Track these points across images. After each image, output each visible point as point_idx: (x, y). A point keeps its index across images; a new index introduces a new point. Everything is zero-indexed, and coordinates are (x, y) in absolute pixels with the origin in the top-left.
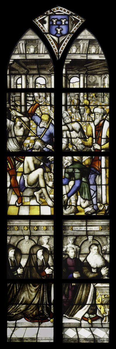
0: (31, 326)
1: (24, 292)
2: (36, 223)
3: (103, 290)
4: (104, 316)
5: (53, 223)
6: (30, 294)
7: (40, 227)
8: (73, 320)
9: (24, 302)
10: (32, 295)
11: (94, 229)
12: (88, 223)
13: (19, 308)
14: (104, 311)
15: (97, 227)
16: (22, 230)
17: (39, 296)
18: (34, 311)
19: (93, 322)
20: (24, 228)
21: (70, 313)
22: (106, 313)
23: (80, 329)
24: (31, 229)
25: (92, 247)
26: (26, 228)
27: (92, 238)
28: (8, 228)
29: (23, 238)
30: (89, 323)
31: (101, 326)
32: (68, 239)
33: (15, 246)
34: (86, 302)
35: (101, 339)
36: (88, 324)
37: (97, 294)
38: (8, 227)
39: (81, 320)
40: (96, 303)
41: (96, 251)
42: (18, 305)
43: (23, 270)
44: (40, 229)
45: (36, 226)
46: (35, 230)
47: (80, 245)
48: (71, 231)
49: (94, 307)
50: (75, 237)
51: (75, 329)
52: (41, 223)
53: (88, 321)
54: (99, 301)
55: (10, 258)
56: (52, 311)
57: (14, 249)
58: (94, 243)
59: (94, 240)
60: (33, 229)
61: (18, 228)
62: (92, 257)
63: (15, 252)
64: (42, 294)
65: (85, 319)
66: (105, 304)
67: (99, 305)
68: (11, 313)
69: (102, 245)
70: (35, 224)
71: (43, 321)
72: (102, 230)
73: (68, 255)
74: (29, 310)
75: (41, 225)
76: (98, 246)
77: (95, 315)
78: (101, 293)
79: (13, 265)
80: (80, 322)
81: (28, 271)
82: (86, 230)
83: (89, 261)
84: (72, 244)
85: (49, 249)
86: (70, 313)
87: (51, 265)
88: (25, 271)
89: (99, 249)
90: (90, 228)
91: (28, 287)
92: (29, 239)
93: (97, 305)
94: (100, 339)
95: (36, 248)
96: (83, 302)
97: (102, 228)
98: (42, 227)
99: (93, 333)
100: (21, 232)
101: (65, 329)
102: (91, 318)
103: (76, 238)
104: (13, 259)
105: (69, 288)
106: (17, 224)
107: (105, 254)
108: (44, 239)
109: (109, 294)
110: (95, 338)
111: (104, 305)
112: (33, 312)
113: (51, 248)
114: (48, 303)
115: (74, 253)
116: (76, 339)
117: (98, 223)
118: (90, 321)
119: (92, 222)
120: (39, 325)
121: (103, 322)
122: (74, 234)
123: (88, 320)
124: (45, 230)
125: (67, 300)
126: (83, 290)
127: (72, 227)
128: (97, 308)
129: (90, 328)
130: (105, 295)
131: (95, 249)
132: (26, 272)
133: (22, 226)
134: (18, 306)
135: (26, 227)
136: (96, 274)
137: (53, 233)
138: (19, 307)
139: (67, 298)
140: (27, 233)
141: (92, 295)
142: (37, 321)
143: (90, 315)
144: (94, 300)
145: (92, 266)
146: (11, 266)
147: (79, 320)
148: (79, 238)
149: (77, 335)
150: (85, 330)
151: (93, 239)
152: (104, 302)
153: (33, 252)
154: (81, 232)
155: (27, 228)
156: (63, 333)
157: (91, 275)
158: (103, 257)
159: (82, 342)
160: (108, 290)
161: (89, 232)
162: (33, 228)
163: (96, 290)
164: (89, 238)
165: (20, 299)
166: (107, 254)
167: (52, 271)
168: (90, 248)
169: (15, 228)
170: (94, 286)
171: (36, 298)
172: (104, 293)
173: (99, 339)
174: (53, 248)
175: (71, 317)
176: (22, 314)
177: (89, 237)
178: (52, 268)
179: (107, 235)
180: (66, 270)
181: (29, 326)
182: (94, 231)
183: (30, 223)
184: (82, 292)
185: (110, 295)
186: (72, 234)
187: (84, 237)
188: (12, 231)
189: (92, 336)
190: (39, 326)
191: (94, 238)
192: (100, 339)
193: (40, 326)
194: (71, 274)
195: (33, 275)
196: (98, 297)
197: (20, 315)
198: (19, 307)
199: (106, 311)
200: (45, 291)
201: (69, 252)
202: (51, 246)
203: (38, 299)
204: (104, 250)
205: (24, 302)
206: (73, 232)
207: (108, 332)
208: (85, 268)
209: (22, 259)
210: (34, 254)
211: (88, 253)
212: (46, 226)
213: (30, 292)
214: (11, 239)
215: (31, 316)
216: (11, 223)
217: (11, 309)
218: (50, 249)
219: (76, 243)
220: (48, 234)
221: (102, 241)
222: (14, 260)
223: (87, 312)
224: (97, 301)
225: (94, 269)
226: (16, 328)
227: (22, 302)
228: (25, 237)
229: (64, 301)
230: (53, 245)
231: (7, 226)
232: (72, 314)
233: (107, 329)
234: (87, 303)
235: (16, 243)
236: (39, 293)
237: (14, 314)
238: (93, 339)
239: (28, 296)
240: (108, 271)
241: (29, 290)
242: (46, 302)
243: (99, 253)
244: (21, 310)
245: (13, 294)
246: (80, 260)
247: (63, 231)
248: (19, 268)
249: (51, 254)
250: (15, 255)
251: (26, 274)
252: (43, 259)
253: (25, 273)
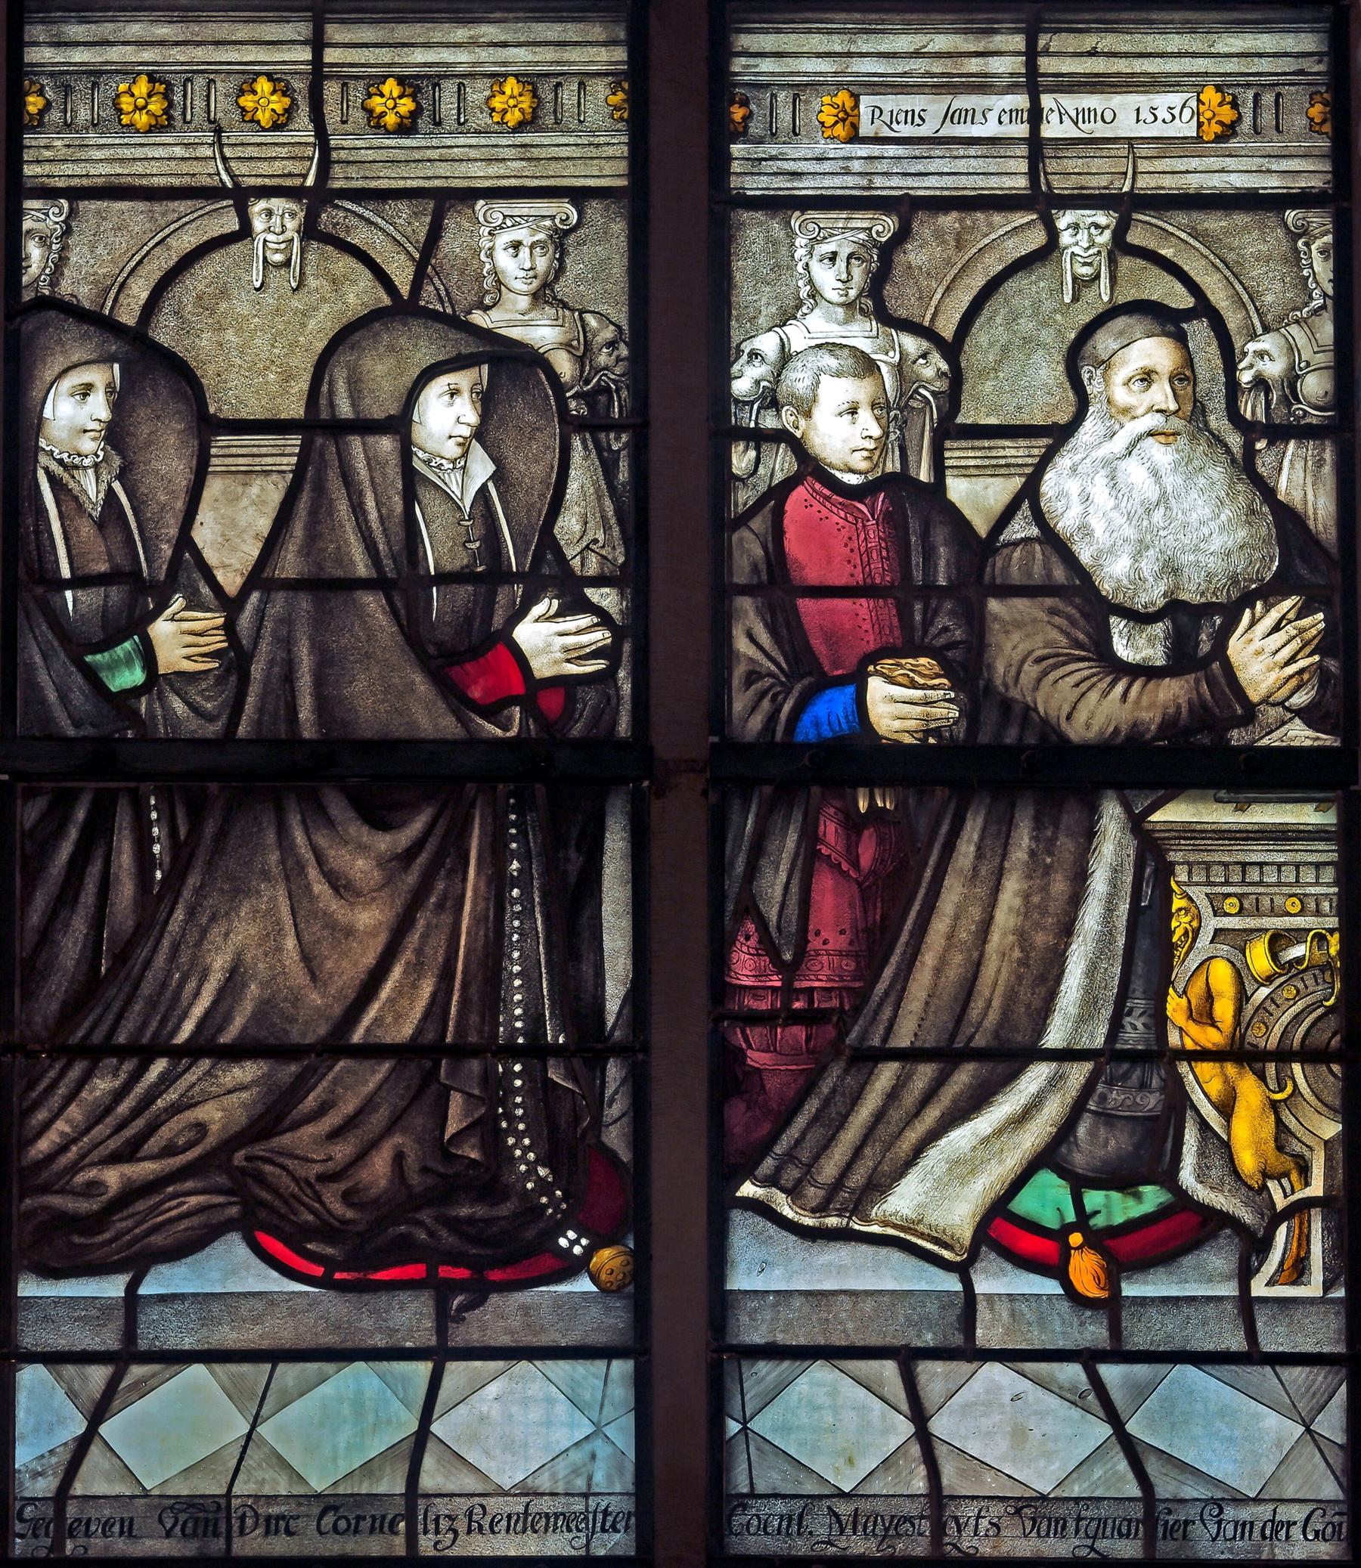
0: (329, 1340)
1: (239, 891)
2: (403, 32)
3: (1254, 875)
4: (1281, 1203)
5: (622, 35)
6: (314, 914)
7: (449, 87)
8: (864, 1248)
9: (238, 1023)
10: (349, 932)
11: (1126, 127)
12: (1047, 53)
13: (176, 1109)
14: (1280, 1148)
15: (1176, 99)
16: (218, 131)
17: (440, 941)
18: (374, 1145)
19: (1129, 1290)
20: (247, 101)
21: (829, 1170)
22: (1304, 1170)
23: (963, 1367)
24: (332, 116)
25: (1104, 342)
26: (267, 102)
27: (1107, 235)
28: (34, 104)
29: (232, 224)
30: (1072, 1293)
31: (1236, 1342)
32: (800, 253)
33: (128, 317)
34: (1040, 1027)
35: (1245, 1514)
36: (1065, 1306)
37: (1180, 924)
38: (41, 93)
39: (973, 1255)
40: (1163, 1036)
41: (1161, 394)
42: (159, 1066)
43: (229, 628)
44: (448, 106)
45: (401, 80)
46: (391, 120)
47: (947, 329)
48: (833, 149)
49: (1143, 1086)
50: (885, 226)
51: (889, 1369)
52: (461, 34)
53: (1058, 1270)
54: (1205, 1015)
55: (52, 478)
56: (615, 1138)
57: (107, 360)
58: (1128, 294)
59: (1126, 263)
60: (358, 115)
61: (167, 96)
62: (1112, 477)
63: (119, 402)
64: (477, 920)
65: (1030, 1244)
66: (1283, 1056)
67: (1205, 1069)
68: (75, 1167)
69: (1233, 321)
70: (385, 55)
71: (495, 1275)
72: (1229, 131)
73: (798, 447)
74: (309, 1130)
75: (462, 57)
76: (1181, 339)
77: (1152, 1197)
78: (1231, 905)
79: (103, 567)
80: (952, 1283)
81: (287, 643)
82: (1022, 130)
83: (1066, 523)
84: (848, 306)
85: (564, 366)
86: (829, 1170)
87: (593, 567)
88: (257, 636)
89: (1202, 370)
90: (1086, 115)
91: (299, 837)
92: (310, 231)
93: (1183, 1068)
94: (1230, 1512)
95: (391, 349)
96: (993, 1017)
97: (1234, 105)
98: (477, 93)
99: (1132, 1427)
100: (209, 153)
101: (763, 1367)
102: (1101, 1240)
103: (902, 236)
104: (91, 487)
105: (810, 837)
106: (148, 55)
107: (1278, 433)
108: (504, 238)
109: (1333, 922)
110: (1165, 1488)
111: (1271, 1069)
112: (361, 1157)
113: (587, 344)
114: (553, 1035)
115: (868, 424)
116: (912, 1509)
117: (1180, 55)
118: (1085, 1269)
119: (1108, 42)
120: (443, 1320)
121: (1259, 1288)
122: (878, 181)
123: (1066, 1251)
124: (520, 127)
125: (788, 991)
126: (999, 874)
127: (843, 97)
128: (1178, 1102)
129: (1089, 1358)
130: (1278, 941)
131: (1147, 377)
132: (264, 647)
133: (210, 73)
134: (166, 1081)
135: (263, 86)
136: (1172, 691)
137: (622, 167)
138: (172, 1096)
139: (790, 970)
140: (278, 167)
141: (1106, 938)
142: (417, 1271)
143: (1093, 1199)
144: (1138, 1002)
145: (1106, 588)
146: (66, 572)
147: (946, 1254)
148: (939, 235)
149: (915, 1450)
150: (1025, 1385)
151: (1120, 246)
152: (1278, 1030)
153: (355, 399)
154: (961, 165)
155: (279, 103)
156: (733, 1427)
157: (1093, 696)
158: (1246, 467)
159: (986, 1550)
160: (1328, 875)
161: (1070, 165)
162: (357, 92)
163: (1169, 869)
164: (1066, 238)
165: (192, 985)
166: (1303, 432)
167: (601, 637)
168: (1074, 358)
169: (126, 102)
170: (1137, 824)
171: (397, 972)
172: (1273, 912)
173: (1218, 1503)
174: (624, 351)
175: (832, 1221)
176: (221, 1180)
177: (1064, 219)
178: (605, 598)
179: (1303, 200)
180: (765, 638)
181: (307, 1342)
182: (1130, 141)
183: (318, 44)
184: (981, 891)
185: (1341, 941)
186: (850, 181)
187: (1003, 222)
188: (92, 138)
189: (1123, 1466)
190: (441, 1330)
191: (1135, 237)
192: (1230, 1512)
193: (459, 1336)
194: (840, 682)
195: (360, 685)
196: (1193, 962)
197: (193, 1201)
198: (182, 1084)
199: (1297, 1148)
200: (523, 880)
201: (806, 408)
202: (592, 321)
203: (427, 988)
204: (1260, 383)
205: (238, 1023)
206: (856, 166)
207: (1332, 1424)
208: (1021, 605)
209: (213, 488)
210: (366, 427)
211: (1063, 417)
212: (530, 80)
213: (320, 888)
214: (67, 232)
215: (338, 1207)
216: (75, 31)
217: (74, 1111)
218: (581, 361)
219: (902, 300)
220: (554, 168)
221: (1233, 272)
222: (110, 493)
223: (1048, 1158)
224: (1175, 1006)
225: (1139, 618)
226: (137, 1371)
227: (221, 1029)
228: (258, 207)
229: (749, 1002)
230: (621, 315)
231: (18, 75)
232: (856, 1179)
233: (1320, 1376)
234: (1054, 1037)
235: (140, 291)
236: (440, 906)
237: (113, 1177)
238: (1137, 1512)
239: (290, 943)
240: (1324, 646)
241: (313, 873)
242: (535, 1020)
243: (1197, 413)
244: (201, 1128)
245: (98, 921)
246: (953, 513)
247: (737, 149)
248: (178, 603)
249: (594, 426)
250: (115, 434)
251: (266, 681)
252: (483, 490)
253: (257, 670)
